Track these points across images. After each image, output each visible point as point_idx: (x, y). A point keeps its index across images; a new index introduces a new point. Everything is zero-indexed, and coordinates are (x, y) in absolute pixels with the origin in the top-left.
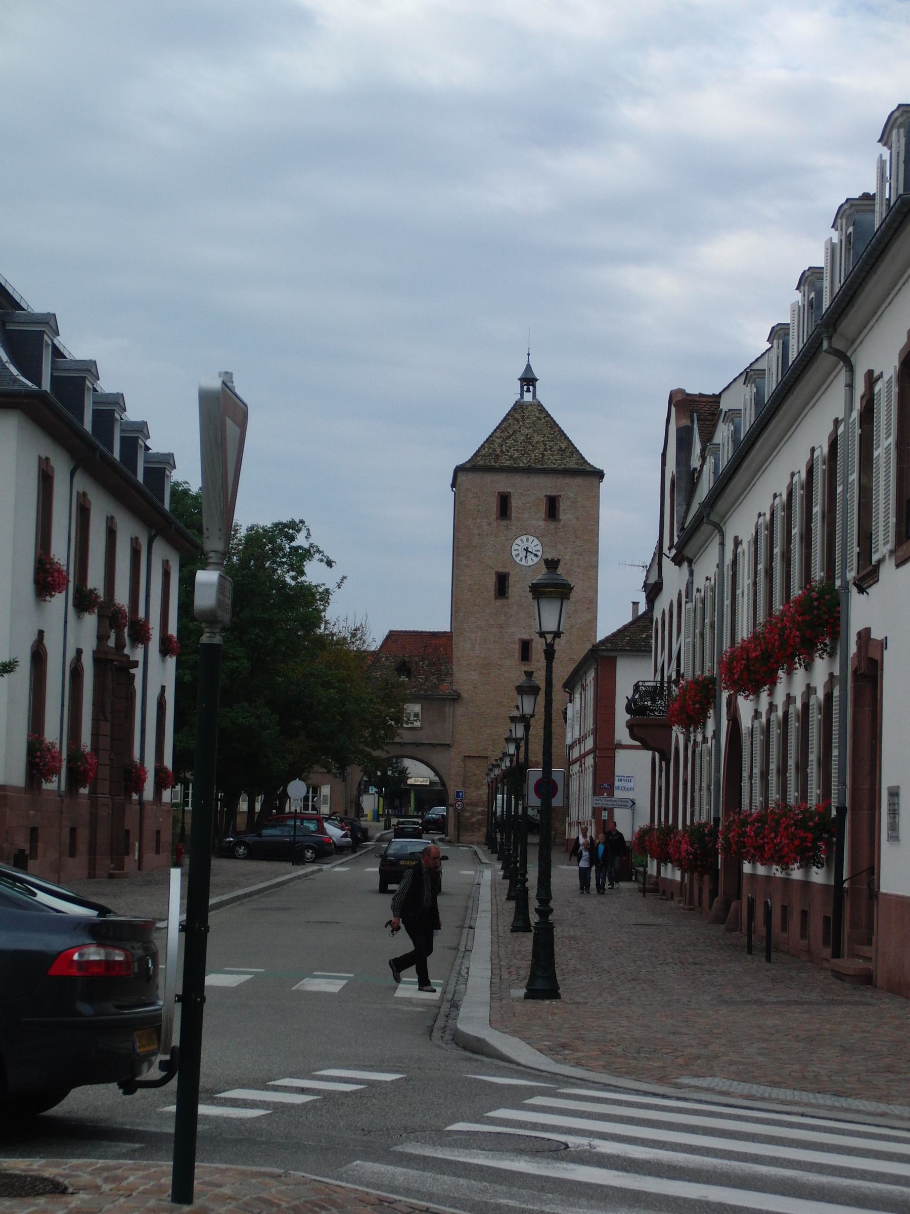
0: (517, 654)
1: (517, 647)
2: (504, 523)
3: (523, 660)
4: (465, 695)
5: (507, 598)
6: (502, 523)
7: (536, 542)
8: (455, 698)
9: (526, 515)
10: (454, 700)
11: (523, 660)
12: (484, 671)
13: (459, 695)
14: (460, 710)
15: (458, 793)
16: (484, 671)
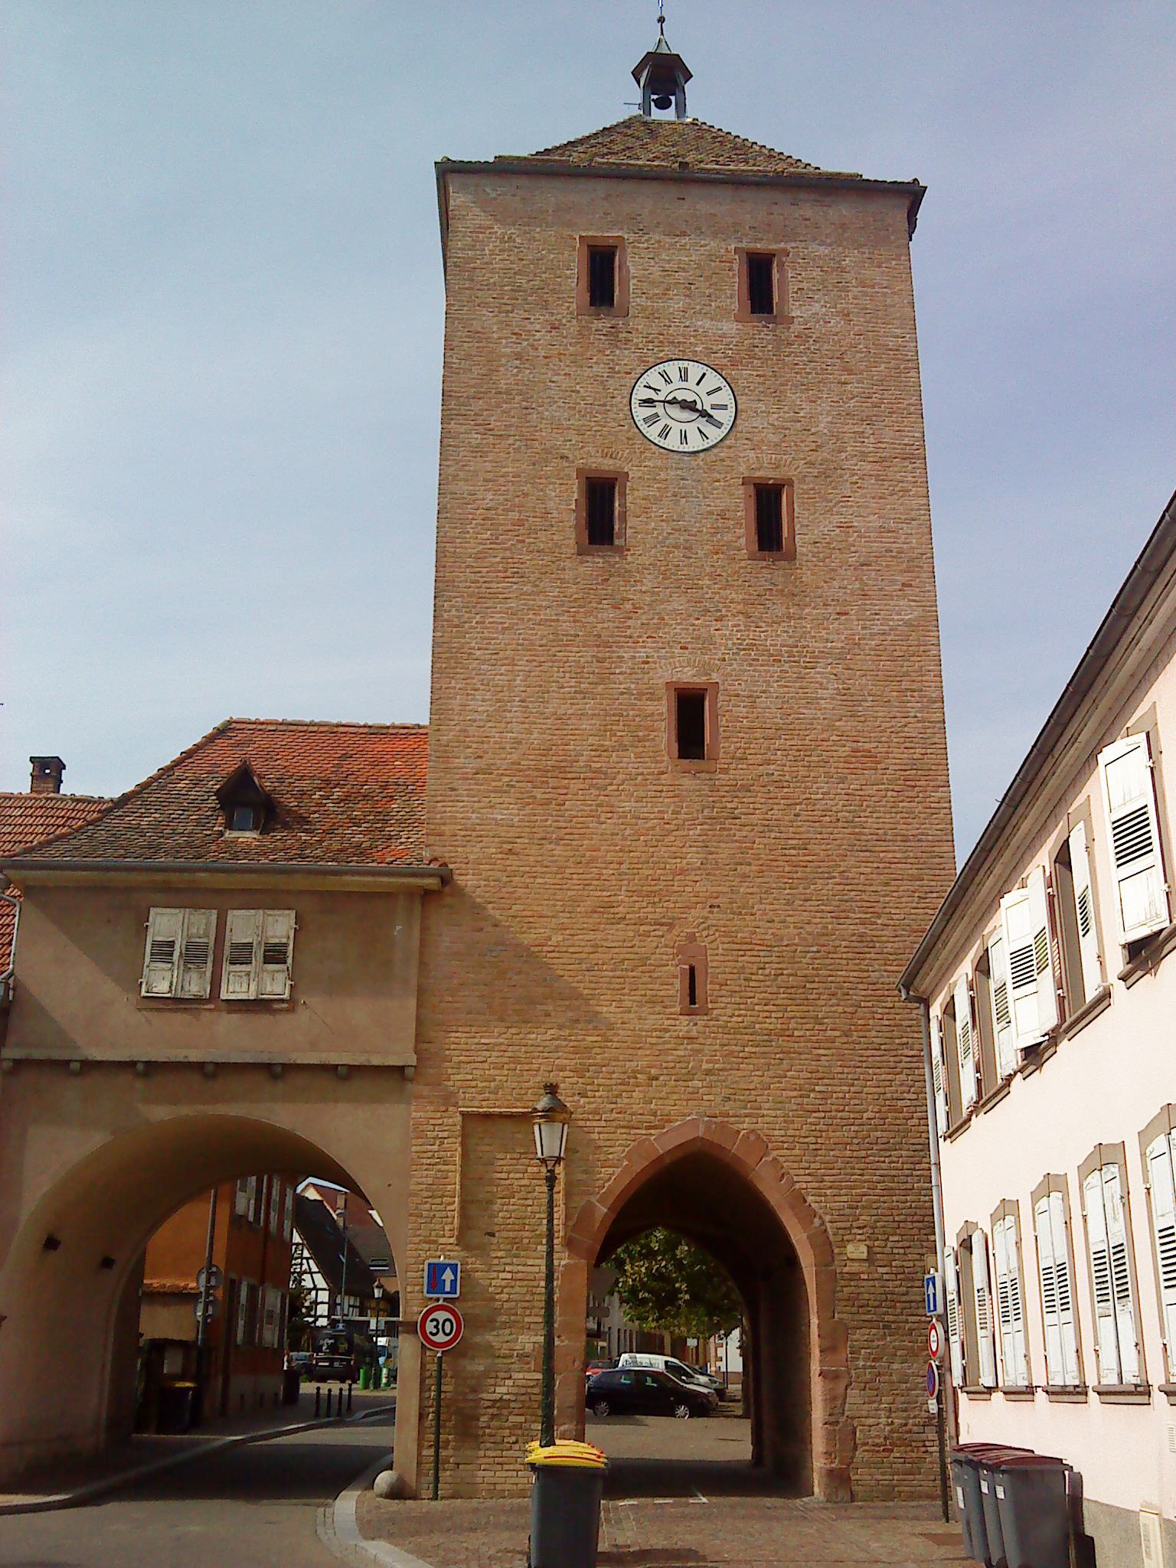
0: (665, 735)
1: (664, 709)
2: (603, 324)
3: (682, 755)
4: (466, 880)
5: (621, 551)
6: (597, 324)
7: (713, 380)
8: (436, 890)
9: (678, 304)
10: (427, 894)
11: (682, 755)
12: (538, 794)
13: (446, 879)
14: (448, 936)
15: (436, 1271)
16: (538, 794)
